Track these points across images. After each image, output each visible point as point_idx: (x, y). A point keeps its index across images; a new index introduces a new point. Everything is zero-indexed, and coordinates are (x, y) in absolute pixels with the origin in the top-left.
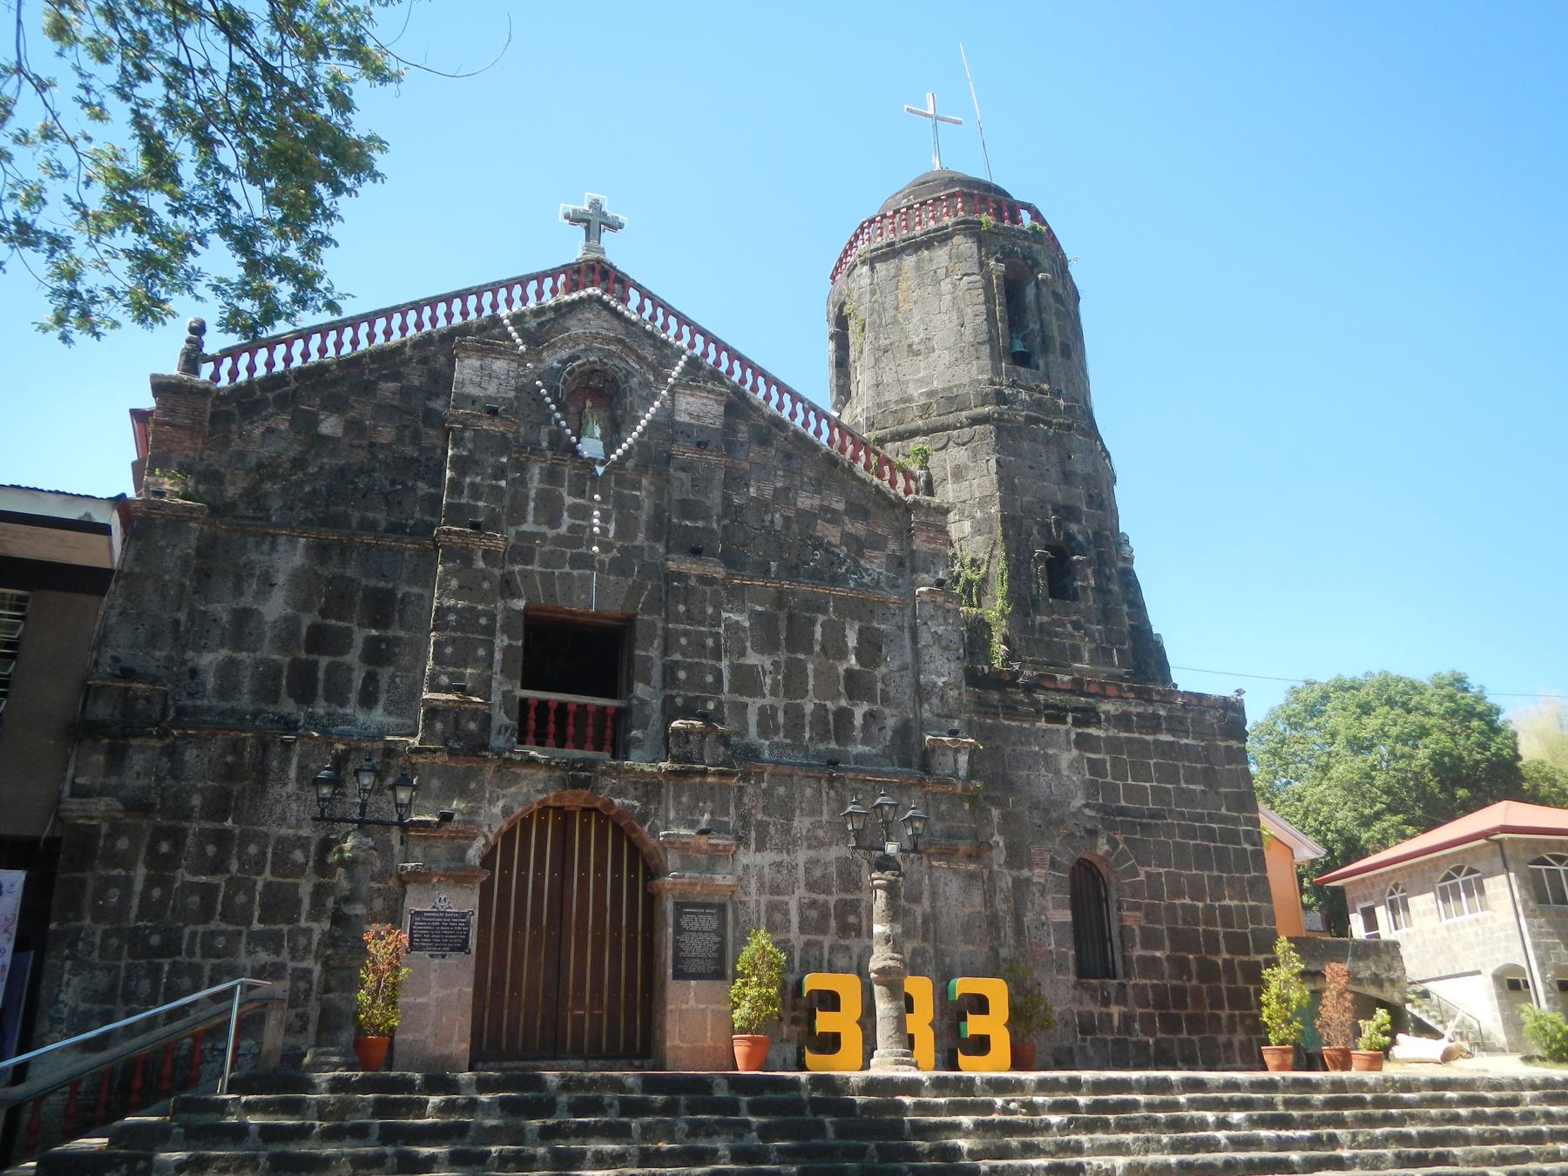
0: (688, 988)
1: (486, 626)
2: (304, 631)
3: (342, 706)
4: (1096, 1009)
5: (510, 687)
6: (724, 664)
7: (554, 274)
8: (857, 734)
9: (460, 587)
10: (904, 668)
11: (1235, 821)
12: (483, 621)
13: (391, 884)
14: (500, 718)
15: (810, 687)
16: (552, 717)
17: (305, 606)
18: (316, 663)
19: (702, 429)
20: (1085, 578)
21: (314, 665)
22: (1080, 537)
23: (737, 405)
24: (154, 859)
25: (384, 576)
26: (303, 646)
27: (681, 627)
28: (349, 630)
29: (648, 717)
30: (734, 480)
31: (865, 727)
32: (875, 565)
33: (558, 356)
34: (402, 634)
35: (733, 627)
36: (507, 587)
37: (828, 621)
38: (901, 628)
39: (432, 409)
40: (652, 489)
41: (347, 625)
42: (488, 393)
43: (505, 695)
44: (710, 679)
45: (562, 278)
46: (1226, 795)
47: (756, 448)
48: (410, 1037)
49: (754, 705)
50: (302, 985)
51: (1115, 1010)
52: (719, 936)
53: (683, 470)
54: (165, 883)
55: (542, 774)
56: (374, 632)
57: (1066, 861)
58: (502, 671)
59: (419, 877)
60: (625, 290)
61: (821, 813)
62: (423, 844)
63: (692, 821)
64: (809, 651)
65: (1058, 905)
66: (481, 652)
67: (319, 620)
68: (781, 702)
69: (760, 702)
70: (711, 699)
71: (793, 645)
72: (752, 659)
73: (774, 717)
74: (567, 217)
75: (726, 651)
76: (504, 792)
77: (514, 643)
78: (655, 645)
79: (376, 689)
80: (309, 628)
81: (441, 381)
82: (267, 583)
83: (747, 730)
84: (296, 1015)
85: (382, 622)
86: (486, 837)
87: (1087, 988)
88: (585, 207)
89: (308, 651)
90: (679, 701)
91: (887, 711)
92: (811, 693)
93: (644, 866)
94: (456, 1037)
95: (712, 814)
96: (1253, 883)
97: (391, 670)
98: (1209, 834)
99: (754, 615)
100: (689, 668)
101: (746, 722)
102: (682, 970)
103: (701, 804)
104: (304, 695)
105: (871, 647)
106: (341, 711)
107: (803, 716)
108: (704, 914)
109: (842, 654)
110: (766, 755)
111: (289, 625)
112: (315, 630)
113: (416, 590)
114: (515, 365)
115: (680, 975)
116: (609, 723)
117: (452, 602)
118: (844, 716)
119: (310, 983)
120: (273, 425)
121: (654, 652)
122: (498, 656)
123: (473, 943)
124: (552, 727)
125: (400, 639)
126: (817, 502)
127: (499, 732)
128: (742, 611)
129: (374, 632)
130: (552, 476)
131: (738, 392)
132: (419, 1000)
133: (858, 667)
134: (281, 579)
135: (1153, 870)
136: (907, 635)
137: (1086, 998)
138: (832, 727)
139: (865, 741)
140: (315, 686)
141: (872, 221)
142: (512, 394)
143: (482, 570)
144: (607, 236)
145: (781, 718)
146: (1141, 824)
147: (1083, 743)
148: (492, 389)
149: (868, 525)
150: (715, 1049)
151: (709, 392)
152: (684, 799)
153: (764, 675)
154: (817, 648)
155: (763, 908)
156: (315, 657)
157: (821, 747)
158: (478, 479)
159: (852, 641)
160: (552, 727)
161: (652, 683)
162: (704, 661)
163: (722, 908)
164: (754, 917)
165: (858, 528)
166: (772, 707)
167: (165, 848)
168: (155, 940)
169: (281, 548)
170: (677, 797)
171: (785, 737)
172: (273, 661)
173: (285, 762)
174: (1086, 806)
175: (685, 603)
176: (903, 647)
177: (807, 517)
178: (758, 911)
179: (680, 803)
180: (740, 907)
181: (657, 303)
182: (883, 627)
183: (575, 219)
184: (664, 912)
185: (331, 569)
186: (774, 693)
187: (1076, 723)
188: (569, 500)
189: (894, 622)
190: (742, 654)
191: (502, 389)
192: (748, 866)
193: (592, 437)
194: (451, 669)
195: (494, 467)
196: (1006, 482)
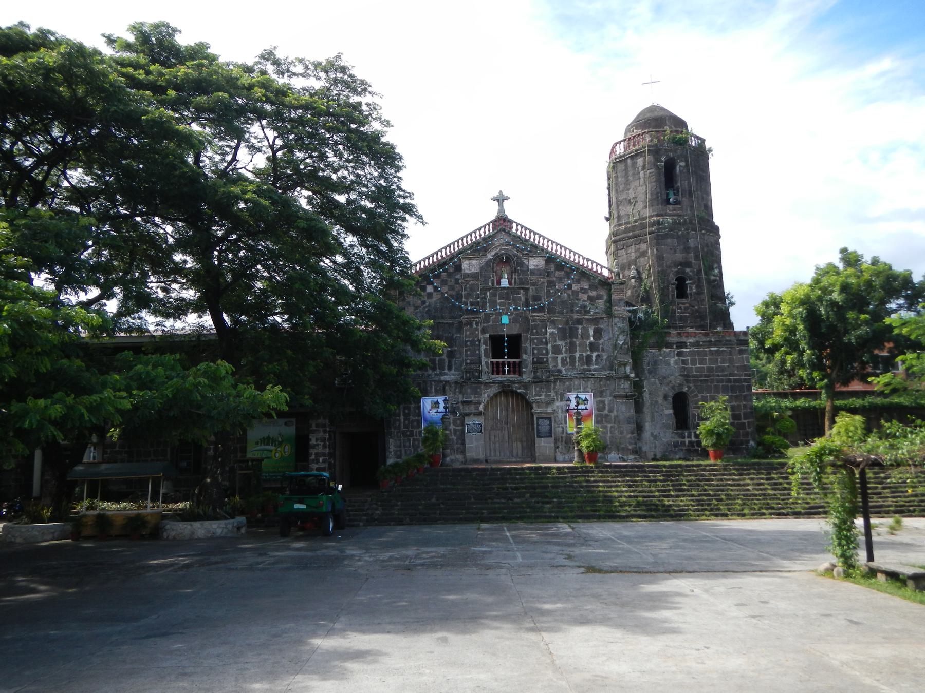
4: (680, 440)
6: (549, 346)
7: (489, 225)
8: (594, 361)
11: (741, 375)
14: (485, 369)
19: (539, 270)
20: (691, 289)
22: (691, 273)
23: (551, 259)
24: (405, 415)
30: (551, 284)
31: (596, 360)
32: (601, 304)
36: (484, 331)
38: (608, 326)
43: (486, 362)
44: (544, 351)
45: (491, 225)
46: (737, 367)
47: (557, 272)
49: (559, 357)
51: (687, 440)
54: (408, 420)
57: (671, 394)
59: (468, 415)
60: (512, 224)
64: (577, 338)
65: (667, 409)
66: (477, 352)
68: (567, 355)
69: (561, 356)
71: (571, 337)
72: (559, 343)
73: (566, 360)
81: (458, 268)
87: (677, 434)
88: (496, 194)
90: (535, 360)
93: (529, 405)
96: (745, 397)
98: (729, 381)
99: (558, 329)
100: (538, 349)
104: (434, 369)
105: (598, 333)
109: (588, 338)
110: (564, 371)
115: (539, 436)
118: (589, 358)
123: (483, 430)
126: (579, 286)
130: (494, 295)
131: (550, 253)
135: (704, 395)
136: (610, 328)
137: (676, 437)
139: (596, 364)
141: (616, 144)
144: (506, 202)
145: (568, 360)
146: (701, 381)
147: (680, 354)
148: (473, 270)
154: (579, 337)
157: (582, 368)
159: (591, 333)
163: (550, 419)
165: (593, 293)
167: (407, 411)
168: (408, 433)
170: (535, 389)
173: (431, 387)
174: (681, 375)
176: (609, 332)
177: (576, 293)
181: (522, 227)
183: (494, 199)
187: (678, 347)
188: (499, 301)
190: (555, 341)
196: (660, 258)
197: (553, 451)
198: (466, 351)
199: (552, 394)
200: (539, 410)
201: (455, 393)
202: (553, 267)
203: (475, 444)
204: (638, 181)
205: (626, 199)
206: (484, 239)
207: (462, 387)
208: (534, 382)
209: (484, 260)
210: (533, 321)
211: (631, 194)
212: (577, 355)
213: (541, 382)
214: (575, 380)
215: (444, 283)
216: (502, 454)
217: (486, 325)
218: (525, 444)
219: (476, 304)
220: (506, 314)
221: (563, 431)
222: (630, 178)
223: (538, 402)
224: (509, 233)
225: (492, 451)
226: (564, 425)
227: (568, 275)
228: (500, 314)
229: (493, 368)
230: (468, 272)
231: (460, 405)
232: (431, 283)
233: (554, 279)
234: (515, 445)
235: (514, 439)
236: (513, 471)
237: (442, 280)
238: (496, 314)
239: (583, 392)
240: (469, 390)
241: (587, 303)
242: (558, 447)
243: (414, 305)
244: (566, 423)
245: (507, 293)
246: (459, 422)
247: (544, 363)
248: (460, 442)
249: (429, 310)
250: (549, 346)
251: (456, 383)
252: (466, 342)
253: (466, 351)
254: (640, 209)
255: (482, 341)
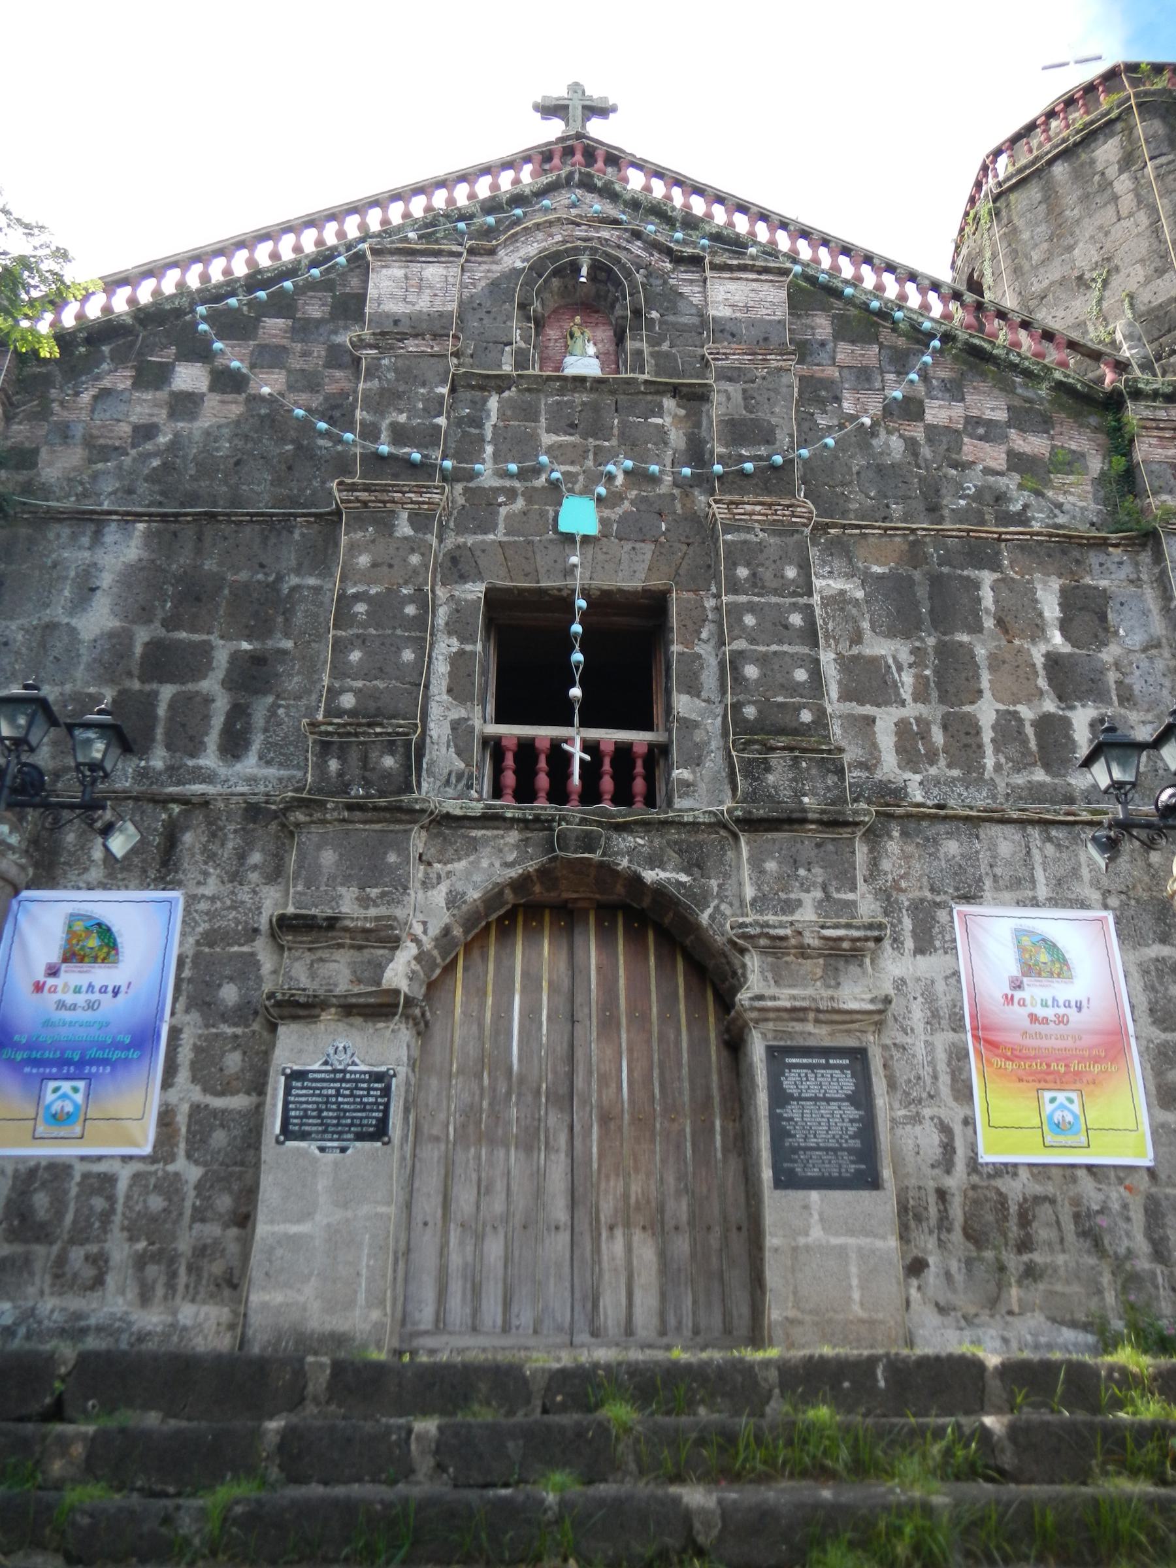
0: (806, 1207)
1: (414, 617)
2: (138, 650)
3: (192, 756)
5: (463, 713)
9: (374, 565)
10: (1153, 645)
12: (410, 610)
13: (256, 1026)
15: (985, 684)
16: (542, 763)
17: (144, 614)
18: (155, 694)
19: (753, 323)
21: (151, 699)
25: (262, 566)
26: (136, 672)
27: (743, 599)
28: (208, 643)
29: (700, 747)
33: (522, 253)
34: (288, 644)
35: (839, 601)
37: (1002, 580)
39: (339, 345)
40: (682, 412)
41: (205, 637)
42: (417, 307)
43: (455, 725)
44: (801, 675)
48: (277, 1297)
49: (886, 720)
50: (99, 1203)
52: (857, 1107)
53: (730, 379)
55: (513, 836)
56: (245, 646)
58: (450, 691)
61: (1033, 881)
62: (308, 957)
63: (787, 902)
64: (976, 628)
66: (408, 655)
67: (162, 632)
68: (933, 711)
70: (804, 706)
71: (943, 619)
73: (925, 735)
74: (538, 108)
75: (827, 637)
76: (449, 867)
77: (469, 648)
78: (704, 635)
79: (247, 730)
80: (147, 644)
82: (86, 591)
83: (879, 761)
84: (87, 1258)
85: (260, 629)
86: (416, 940)
89: (143, 682)
90: (750, 712)
91: (1133, 716)
92: (987, 694)
94: (361, 1298)
95: (824, 888)
97: (270, 699)
100: (763, 660)
101: (875, 746)
102: (792, 1171)
103: (802, 872)
106: (190, 763)
107: (979, 732)
108: (827, 1066)
109: (1037, 630)
111: (118, 642)
112: (155, 647)
113: (312, 581)
114: (455, 270)
115: (787, 1180)
116: (639, 768)
117: (361, 588)
119: (111, 1199)
120: (109, 385)
121: (705, 650)
122: (441, 667)
124: (543, 781)
125: (285, 652)
127: (447, 783)
128: (849, 576)
129: (245, 646)
132: (294, 1229)
133: (1067, 649)
134: (106, 580)
138: (1033, 745)
140: (152, 728)
142: (453, 307)
143: (406, 538)
145: (938, 737)
148: (423, 303)
149: (1052, 438)
150: (871, 1323)
151: (759, 273)
152: (771, 866)
153: (900, 669)
154: (989, 623)
155: (941, 1056)
156: (155, 686)
157: (1020, 780)
158: (402, 418)
159: (1051, 609)
160: (543, 781)
161: (704, 695)
162: (786, 648)
163: (858, 1057)
164: (926, 1072)
165: (1034, 444)
166: (918, 720)
169: (109, 538)
170: (757, 863)
171: (949, 766)
172: (90, 695)
175: (748, 565)
176: (1146, 613)
178: (932, 1063)
179: (762, 872)
180: (897, 1055)
182: (1103, 583)
183: (550, 110)
184: (751, 1065)
185: (183, 560)
186: (920, 696)
189: (1122, 575)
190: (857, 638)
191: (438, 300)
192: (903, 980)
193: (584, 354)
194: (359, 684)
195: (426, 400)
197: (890, 1283)
198: (341, 647)
199: (867, 906)
200: (785, 997)
201: (235, 877)
202: (822, 326)
203: (326, 1215)
204: (1110, 211)
205: (1063, 281)
206: (492, 206)
207: (289, 832)
208: (751, 824)
209: (483, 272)
210: (727, 529)
211: (1084, 256)
212: (986, 712)
213: (792, 821)
214: (996, 830)
215: (270, 357)
216: (525, 1317)
217: (470, 540)
218: (682, 1246)
219: (430, 437)
220: (587, 491)
221: (948, 1148)
222: (1071, 214)
223: (775, 946)
224: (609, 193)
225: (456, 1288)
226: (953, 1114)
227: (900, 362)
228: (555, 493)
229: (498, 771)
230: (394, 307)
231: (262, 949)
232: (200, 352)
233: (833, 372)
234: (614, 1248)
235: (607, 1208)
236: (619, 1412)
237: (263, 348)
238: (531, 495)
239: (1054, 902)
240: (328, 857)
241: (1010, 483)
242: (916, 1267)
243: (89, 442)
244: (963, 1093)
245: (595, 408)
246: (233, 1061)
247: (801, 730)
248: (224, 1202)
249: (167, 467)
250: (827, 657)
251: (254, 812)
252: (345, 602)
253: (341, 647)
254: (1132, 286)
255: (443, 614)
